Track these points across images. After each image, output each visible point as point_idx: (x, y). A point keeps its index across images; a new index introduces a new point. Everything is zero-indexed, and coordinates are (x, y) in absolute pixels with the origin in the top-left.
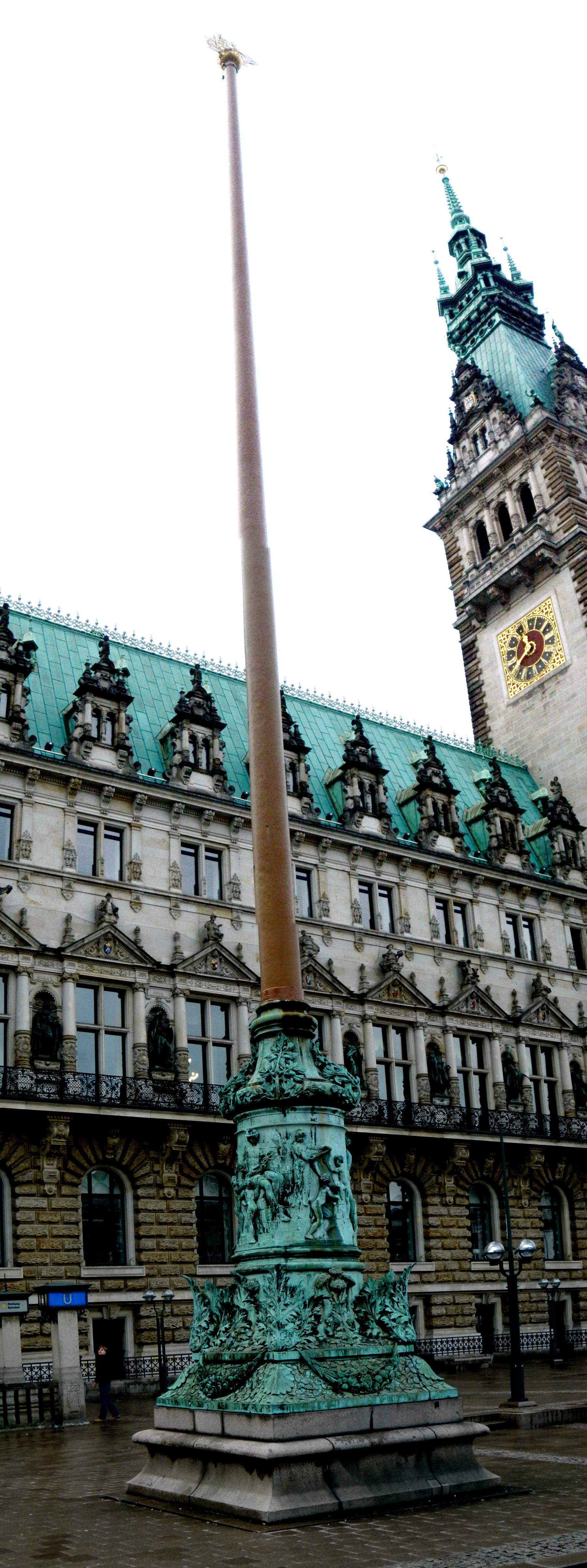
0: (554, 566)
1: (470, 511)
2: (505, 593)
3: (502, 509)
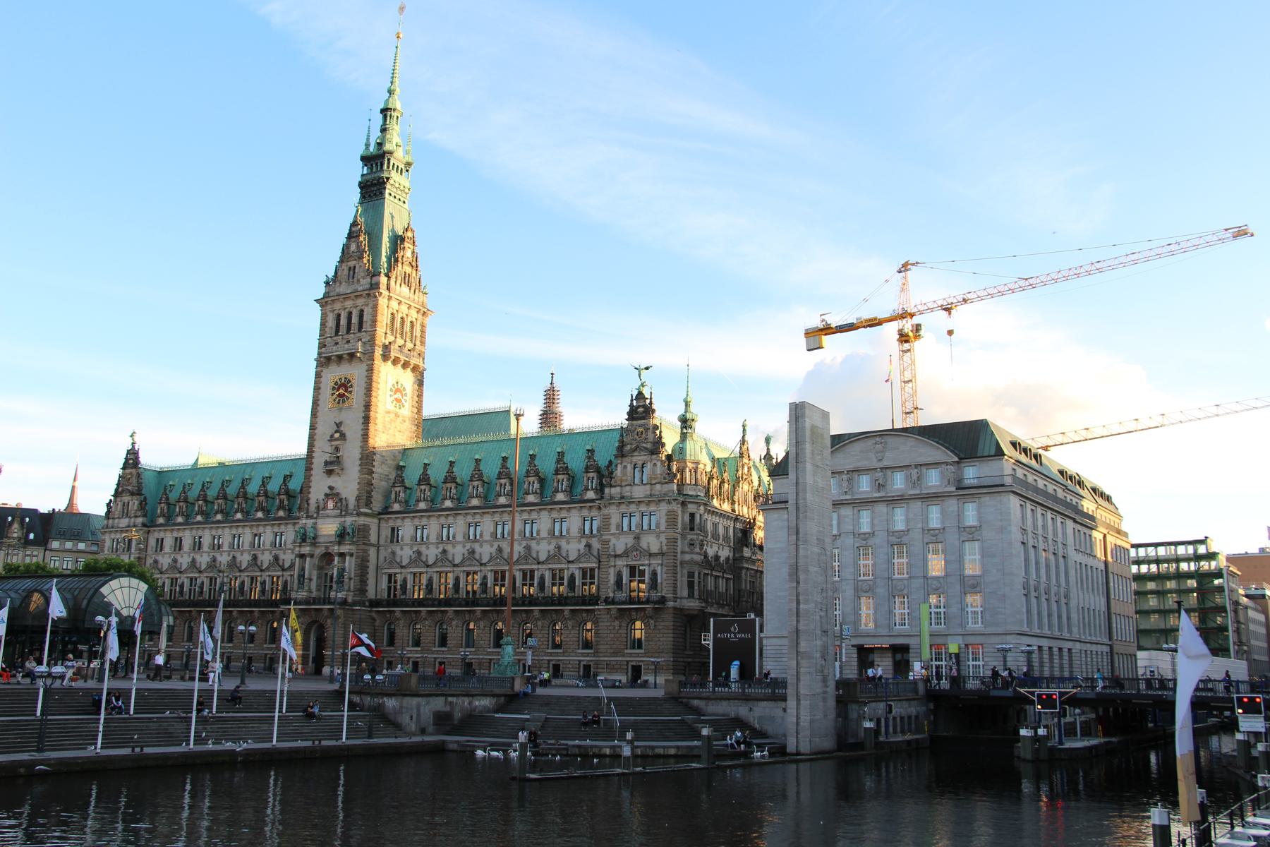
1: (337, 306)
3: (350, 313)
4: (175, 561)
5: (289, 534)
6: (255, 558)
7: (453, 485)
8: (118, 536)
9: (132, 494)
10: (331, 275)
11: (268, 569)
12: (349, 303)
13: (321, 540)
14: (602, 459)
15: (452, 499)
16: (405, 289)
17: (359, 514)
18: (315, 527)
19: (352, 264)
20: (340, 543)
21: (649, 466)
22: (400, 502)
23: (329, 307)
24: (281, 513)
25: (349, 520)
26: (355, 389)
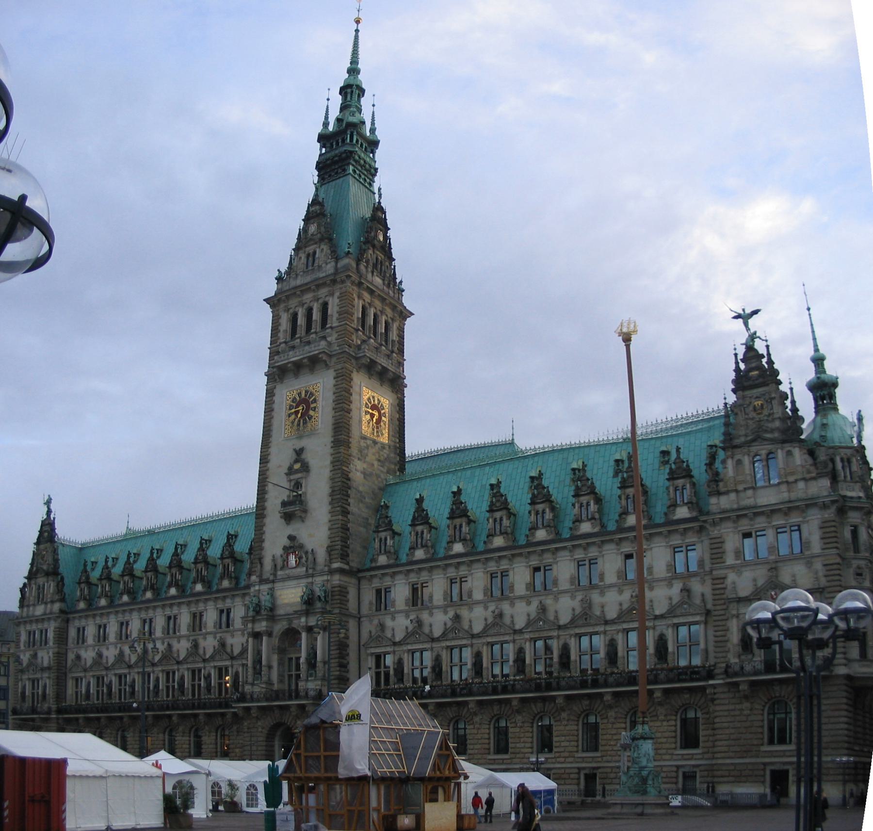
0: (327, 365)
2: (297, 368)
3: (310, 311)
4: (100, 655)
5: (239, 612)
6: (196, 645)
7: (464, 521)
8: (34, 627)
9: (47, 574)
10: (284, 268)
11: (212, 658)
12: (308, 297)
13: (281, 611)
14: (695, 457)
15: (463, 540)
16: (378, 281)
17: (331, 572)
18: (272, 593)
19: (310, 249)
20: (307, 613)
21: (780, 454)
22: (386, 552)
23: (282, 306)
24: (226, 583)
25: (319, 580)
26: (320, 404)
